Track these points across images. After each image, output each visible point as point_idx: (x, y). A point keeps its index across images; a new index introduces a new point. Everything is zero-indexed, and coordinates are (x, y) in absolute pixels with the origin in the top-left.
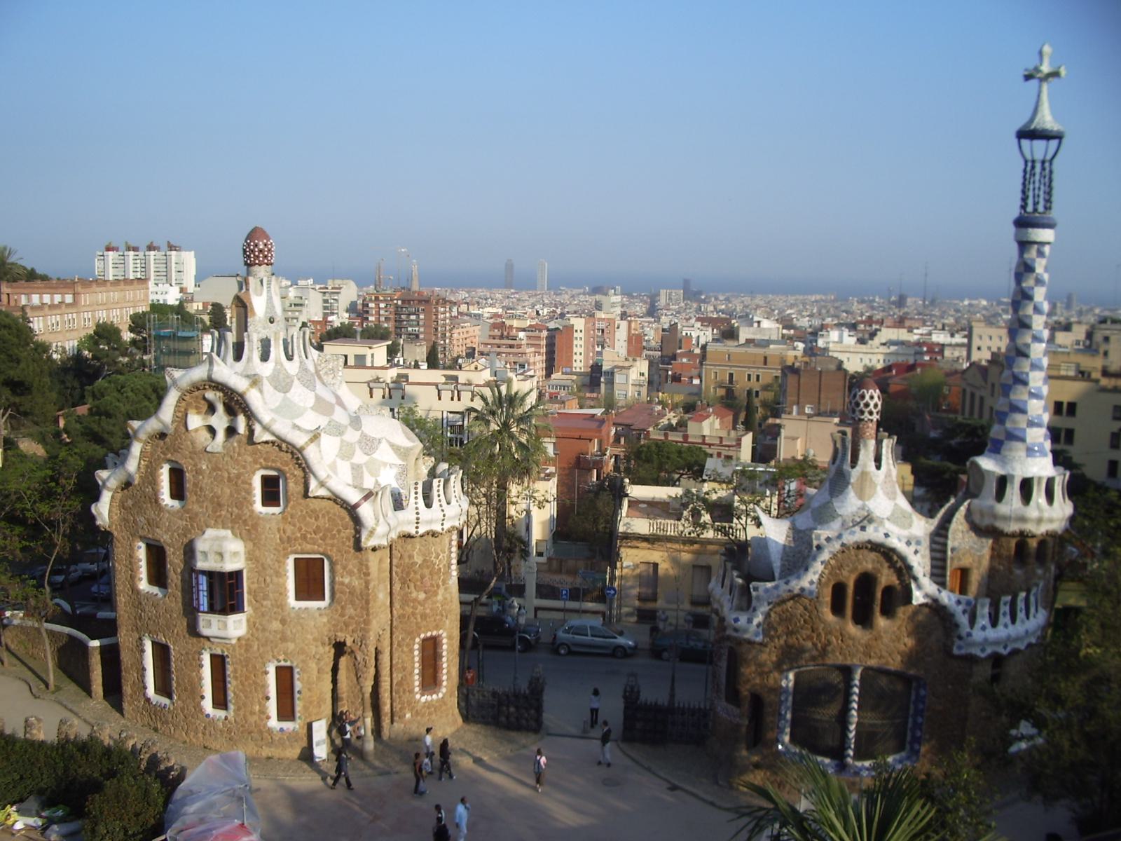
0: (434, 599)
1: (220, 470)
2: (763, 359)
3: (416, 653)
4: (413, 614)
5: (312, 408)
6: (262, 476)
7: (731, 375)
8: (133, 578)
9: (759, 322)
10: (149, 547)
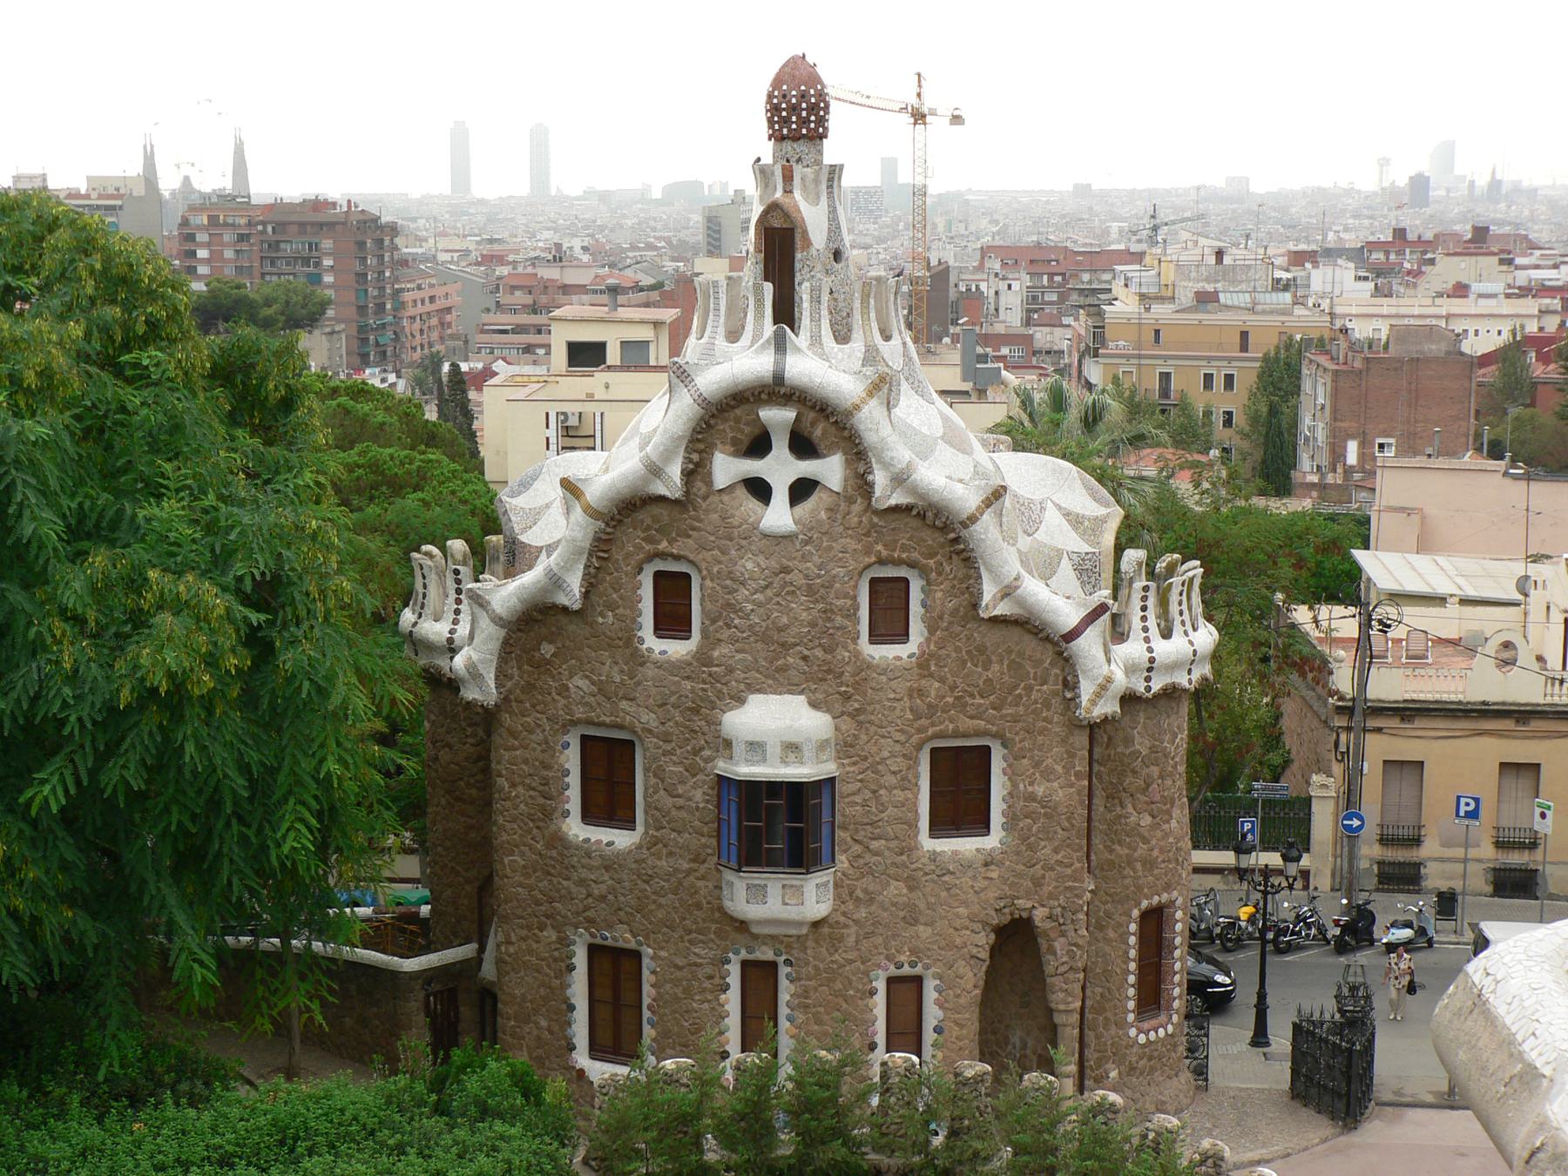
0: (1166, 826)
1: (786, 570)
2: (1238, 339)
3: (1132, 940)
4: (1130, 862)
5: (942, 438)
6: (873, 581)
7: (1165, 377)
8: (548, 811)
9: (1220, 254)
10: (585, 739)
